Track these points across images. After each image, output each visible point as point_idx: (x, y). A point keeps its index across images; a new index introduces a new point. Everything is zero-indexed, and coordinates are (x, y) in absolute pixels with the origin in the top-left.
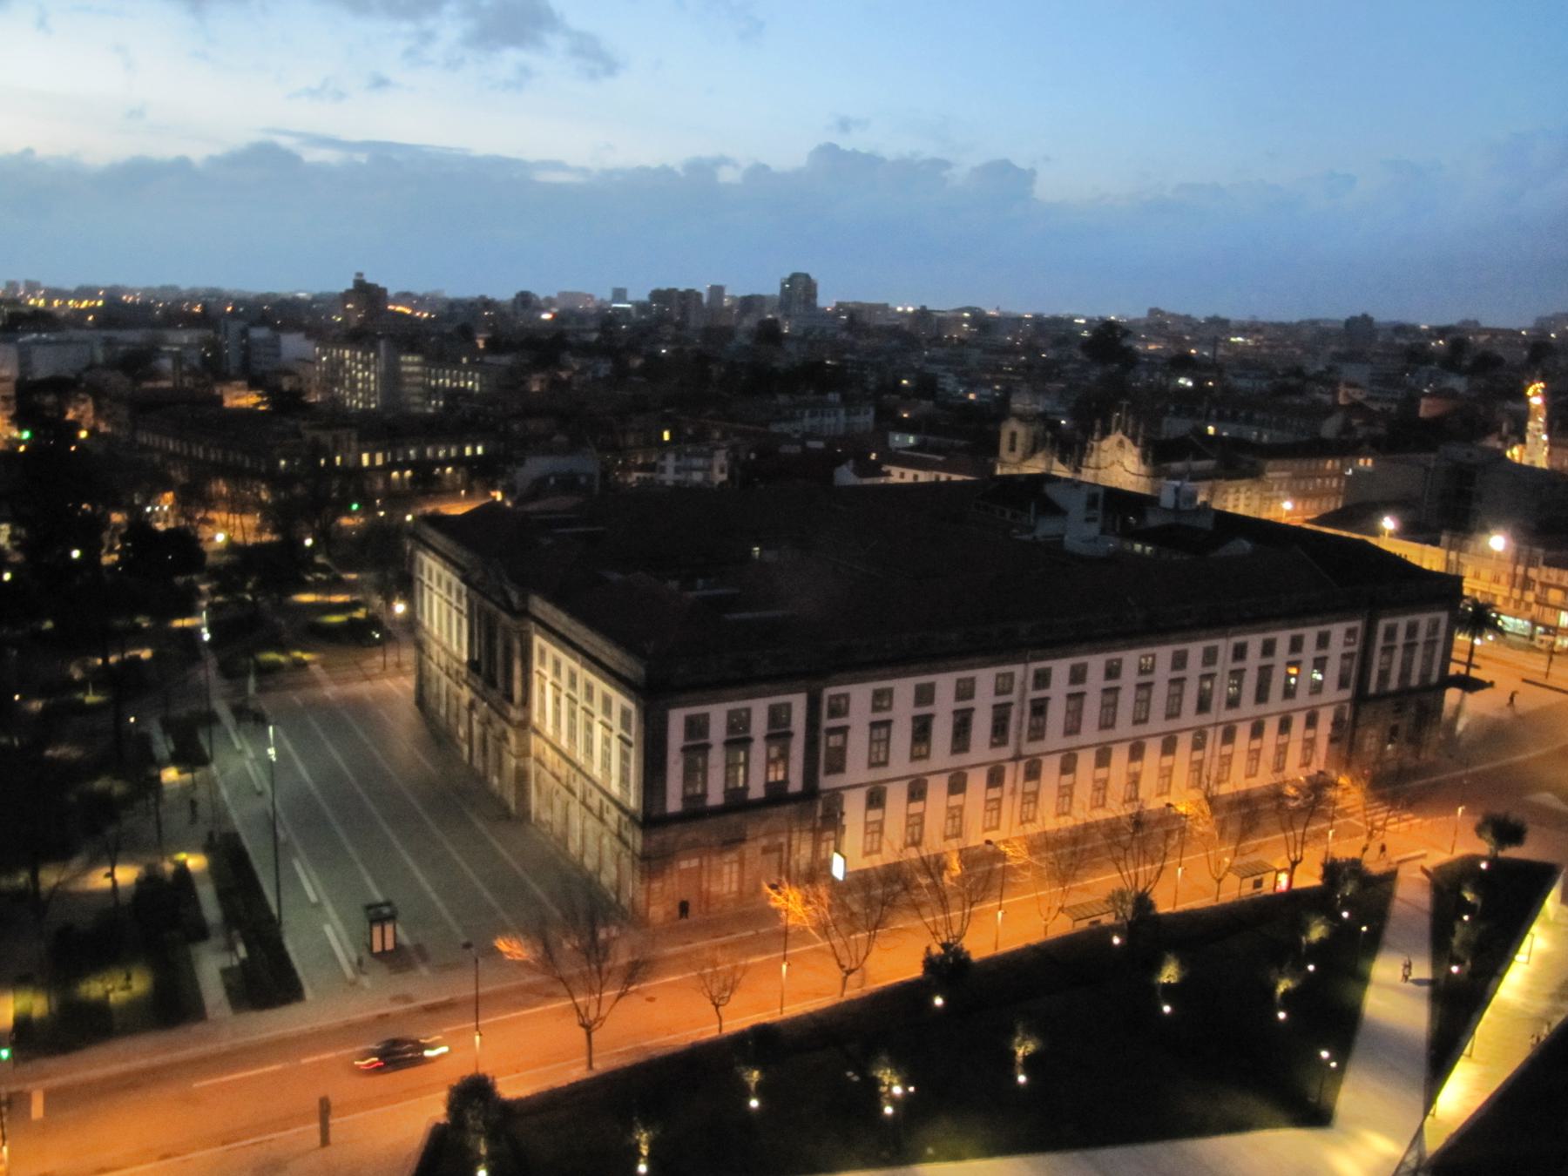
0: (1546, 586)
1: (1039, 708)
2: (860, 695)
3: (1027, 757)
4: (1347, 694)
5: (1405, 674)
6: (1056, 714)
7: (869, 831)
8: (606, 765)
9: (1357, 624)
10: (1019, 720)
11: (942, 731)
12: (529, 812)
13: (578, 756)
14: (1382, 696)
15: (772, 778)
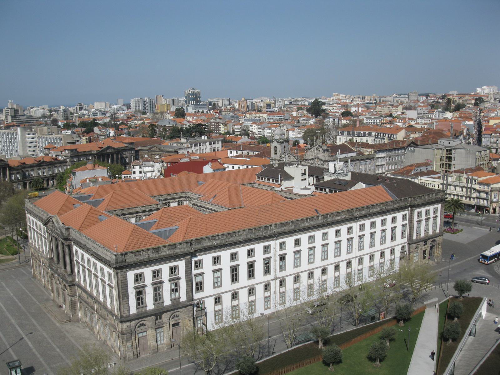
0: (479, 192)
1: (282, 258)
2: (207, 259)
3: (279, 278)
4: (406, 240)
5: (426, 231)
6: (290, 259)
7: (217, 314)
8: (105, 296)
9: (407, 212)
10: (275, 264)
11: (243, 272)
12: (79, 318)
13: (94, 294)
14: (418, 241)
15: (173, 297)
